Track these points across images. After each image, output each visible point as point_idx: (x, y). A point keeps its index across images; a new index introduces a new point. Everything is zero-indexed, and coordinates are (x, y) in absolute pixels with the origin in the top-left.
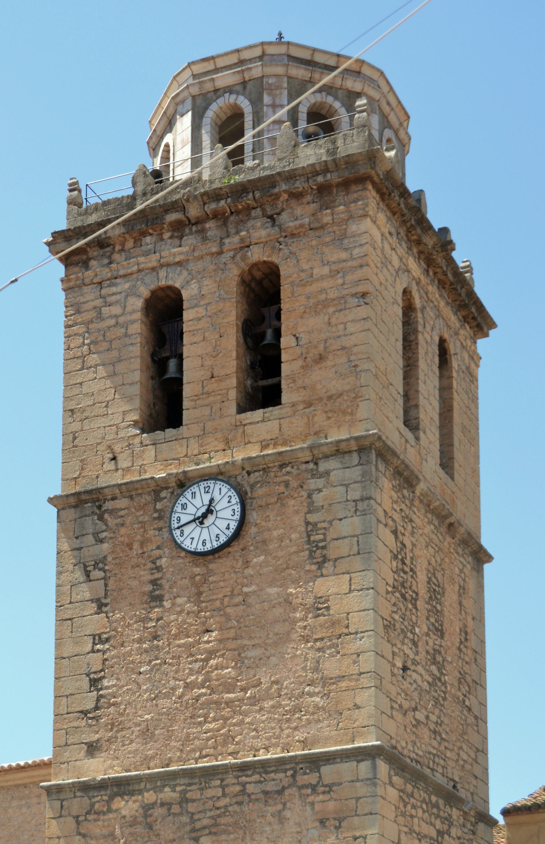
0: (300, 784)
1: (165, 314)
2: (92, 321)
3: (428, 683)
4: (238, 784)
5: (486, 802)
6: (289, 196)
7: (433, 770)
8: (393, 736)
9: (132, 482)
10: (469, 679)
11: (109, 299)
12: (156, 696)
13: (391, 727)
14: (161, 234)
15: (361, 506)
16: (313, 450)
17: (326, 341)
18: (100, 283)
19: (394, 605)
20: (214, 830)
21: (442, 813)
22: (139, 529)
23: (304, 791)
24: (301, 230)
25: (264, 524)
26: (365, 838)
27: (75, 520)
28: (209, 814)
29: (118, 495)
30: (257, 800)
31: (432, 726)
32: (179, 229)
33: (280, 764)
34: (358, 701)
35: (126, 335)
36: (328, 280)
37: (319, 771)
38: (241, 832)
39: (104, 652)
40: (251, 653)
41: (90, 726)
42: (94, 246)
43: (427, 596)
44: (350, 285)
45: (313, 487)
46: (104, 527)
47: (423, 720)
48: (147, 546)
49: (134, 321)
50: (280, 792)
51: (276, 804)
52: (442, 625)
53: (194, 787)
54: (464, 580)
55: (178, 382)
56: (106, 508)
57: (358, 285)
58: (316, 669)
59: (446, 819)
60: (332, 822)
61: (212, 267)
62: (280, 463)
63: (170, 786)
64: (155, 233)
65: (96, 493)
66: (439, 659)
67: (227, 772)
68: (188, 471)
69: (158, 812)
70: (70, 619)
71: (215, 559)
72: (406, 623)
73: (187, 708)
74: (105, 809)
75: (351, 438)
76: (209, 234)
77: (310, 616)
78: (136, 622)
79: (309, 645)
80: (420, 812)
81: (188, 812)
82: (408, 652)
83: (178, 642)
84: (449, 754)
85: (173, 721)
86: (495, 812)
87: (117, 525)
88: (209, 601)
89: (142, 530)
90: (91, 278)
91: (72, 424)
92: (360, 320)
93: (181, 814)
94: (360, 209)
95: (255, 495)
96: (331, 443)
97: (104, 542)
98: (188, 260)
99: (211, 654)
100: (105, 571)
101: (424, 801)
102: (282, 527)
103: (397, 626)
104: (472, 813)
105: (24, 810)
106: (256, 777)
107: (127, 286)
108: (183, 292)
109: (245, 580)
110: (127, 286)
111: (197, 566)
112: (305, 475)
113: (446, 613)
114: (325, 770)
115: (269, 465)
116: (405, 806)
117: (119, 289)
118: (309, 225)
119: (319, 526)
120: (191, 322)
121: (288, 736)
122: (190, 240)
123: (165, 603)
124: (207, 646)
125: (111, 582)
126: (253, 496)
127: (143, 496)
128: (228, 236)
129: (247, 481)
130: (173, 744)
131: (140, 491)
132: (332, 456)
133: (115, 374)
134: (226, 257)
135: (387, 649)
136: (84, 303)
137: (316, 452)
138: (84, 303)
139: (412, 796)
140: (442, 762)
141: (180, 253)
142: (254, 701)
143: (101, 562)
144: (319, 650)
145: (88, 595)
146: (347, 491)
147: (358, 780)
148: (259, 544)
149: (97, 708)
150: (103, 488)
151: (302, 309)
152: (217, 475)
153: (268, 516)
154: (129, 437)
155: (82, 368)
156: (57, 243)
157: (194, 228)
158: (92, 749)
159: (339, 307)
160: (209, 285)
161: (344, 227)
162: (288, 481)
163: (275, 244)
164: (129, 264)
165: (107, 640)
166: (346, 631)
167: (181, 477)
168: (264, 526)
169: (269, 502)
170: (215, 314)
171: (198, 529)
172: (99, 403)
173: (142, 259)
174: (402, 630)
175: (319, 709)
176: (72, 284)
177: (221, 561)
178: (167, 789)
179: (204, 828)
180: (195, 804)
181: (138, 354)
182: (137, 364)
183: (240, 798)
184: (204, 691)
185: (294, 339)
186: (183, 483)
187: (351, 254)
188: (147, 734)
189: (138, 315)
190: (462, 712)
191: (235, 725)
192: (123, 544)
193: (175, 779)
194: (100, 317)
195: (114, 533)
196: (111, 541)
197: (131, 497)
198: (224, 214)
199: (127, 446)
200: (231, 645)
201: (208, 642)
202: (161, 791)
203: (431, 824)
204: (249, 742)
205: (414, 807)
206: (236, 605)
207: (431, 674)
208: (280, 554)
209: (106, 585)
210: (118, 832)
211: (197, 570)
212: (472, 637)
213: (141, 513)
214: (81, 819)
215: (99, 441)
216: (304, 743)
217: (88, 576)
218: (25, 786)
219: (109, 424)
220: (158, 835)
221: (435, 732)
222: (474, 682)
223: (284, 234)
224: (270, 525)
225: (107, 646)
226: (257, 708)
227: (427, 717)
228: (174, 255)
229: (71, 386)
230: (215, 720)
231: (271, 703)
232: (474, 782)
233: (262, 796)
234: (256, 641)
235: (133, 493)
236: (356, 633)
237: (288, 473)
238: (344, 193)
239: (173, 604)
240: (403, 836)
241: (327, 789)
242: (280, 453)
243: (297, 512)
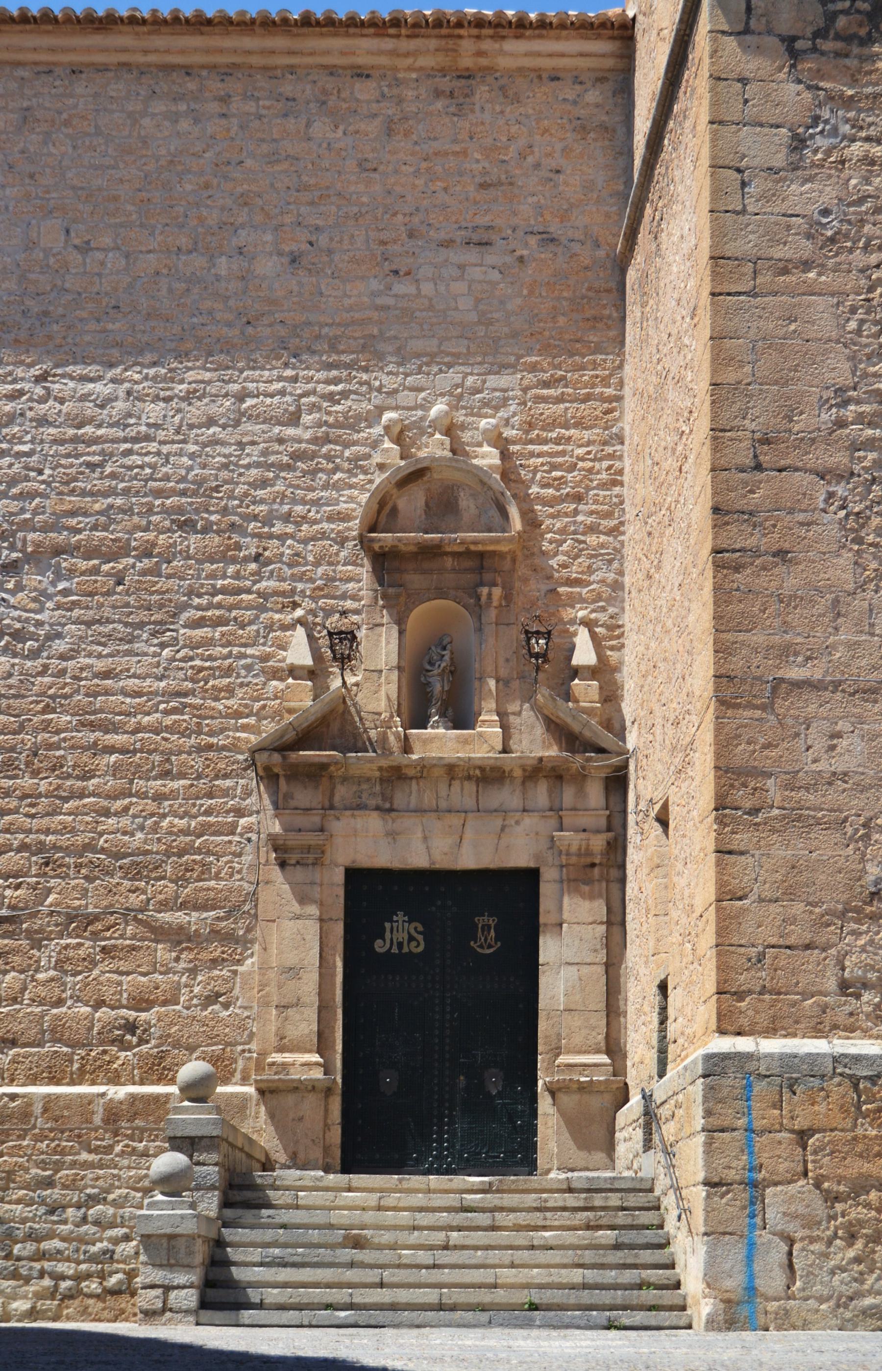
74: (863, 32)
214: (799, 45)
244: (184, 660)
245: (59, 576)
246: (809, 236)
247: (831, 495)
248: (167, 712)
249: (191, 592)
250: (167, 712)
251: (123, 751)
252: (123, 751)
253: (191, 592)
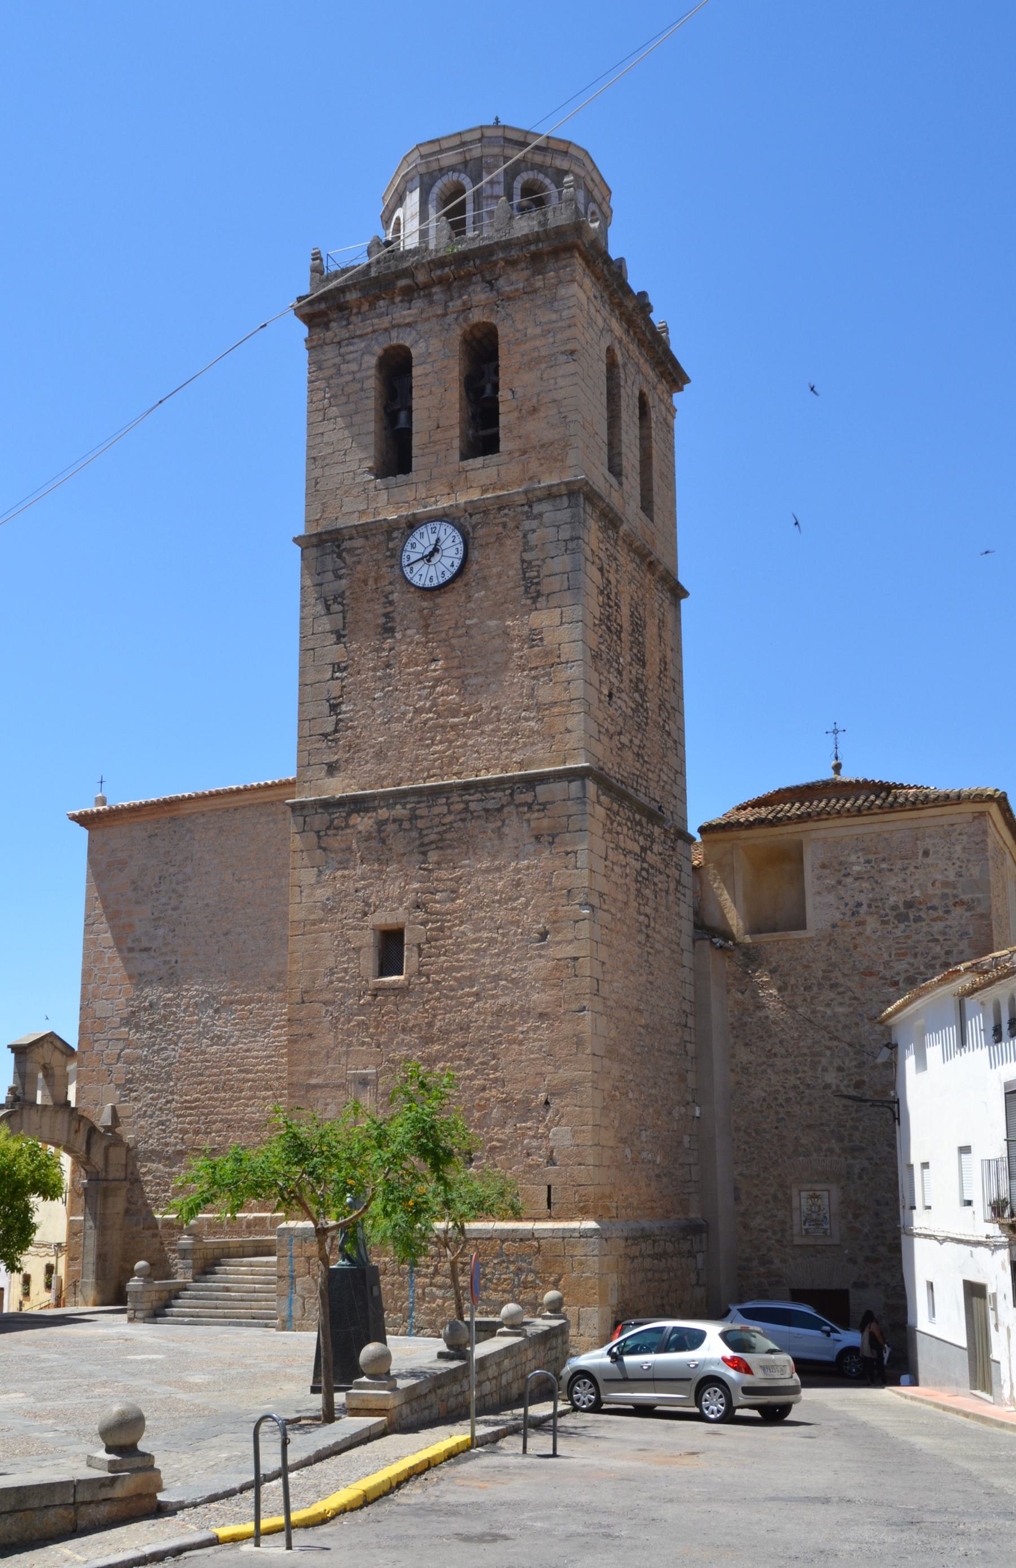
0: (517, 802)
1: (396, 369)
2: (332, 377)
3: (632, 709)
4: (462, 802)
5: (685, 820)
7: (636, 790)
8: (601, 758)
9: (367, 523)
10: (668, 706)
11: (347, 357)
12: (389, 720)
13: (599, 750)
14: (393, 298)
15: (570, 545)
17: (538, 394)
18: (339, 343)
19: (601, 636)
20: (440, 845)
21: (645, 831)
23: (521, 809)
25: (484, 562)
26: (576, 853)
28: (436, 830)
30: (479, 817)
31: (636, 749)
32: (409, 294)
33: (499, 783)
34: (569, 725)
35: (362, 390)
37: (534, 791)
38: (464, 847)
39: (343, 679)
40: (474, 681)
41: (330, 748)
43: (630, 629)
45: (527, 527)
46: (343, 565)
47: (627, 743)
49: (368, 378)
50: (500, 810)
51: (495, 821)
52: (643, 656)
53: (423, 805)
54: (663, 614)
55: (408, 433)
58: (531, 696)
59: (648, 836)
60: (547, 838)
61: (437, 328)
63: (401, 803)
66: (641, 687)
67: (452, 791)
69: (391, 827)
70: (313, 649)
72: (611, 654)
73: (416, 731)
74: (343, 825)
77: (526, 646)
78: (371, 652)
79: (525, 673)
80: (625, 828)
81: (417, 828)
82: (614, 680)
83: (408, 670)
84: (650, 775)
85: (404, 743)
86: (693, 830)
87: (354, 562)
93: (410, 830)
96: (544, 487)
98: (416, 322)
99: (438, 681)
100: (343, 605)
101: (628, 819)
102: (501, 564)
103: (604, 656)
104: (672, 831)
105: (271, 825)
106: (478, 796)
107: (363, 345)
108: (412, 351)
110: (363, 345)
111: (425, 600)
113: (648, 645)
114: (540, 789)
116: (612, 824)
121: (507, 758)
122: (418, 304)
123: (396, 635)
124: (434, 674)
125: (349, 615)
128: (452, 300)
130: (404, 764)
131: (374, 532)
133: (352, 425)
134: (451, 318)
135: (594, 677)
137: (530, 496)
139: (618, 814)
140: (644, 783)
141: (410, 315)
142: (476, 724)
143: (340, 596)
144: (534, 678)
145: (328, 627)
147: (569, 799)
149: (336, 731)
150: (341, 529)
152: (443, 517)
155: (324, 420)
157: (422, 293)
158: (332, 769)
159: (550, 364)
160: (435, 344)
165: (345, 668)
166: (558, 660)
167: (410, 518)
170: (440, 370)
171: (426, 566)
173: (376, 321)
174: (608, 660)
175: (534, 732)
176: (314, 343)
178: (398, 807)
179: (432, 843)
180: (423, 821)
181: (373, 406)
182: (371, 416)
183: (463, 816)
184: (431, 715)
185: (510, 393)
186: (413, 524)
188: (380, 755)
189: (373, 372)
190: (662, 736)
191: (459, 747)
193: (405, 797)
197: (366, 538)
200: (456, 673)
201: (435, 670)
202: (393, 808)
203: (635, 841)
204: (472, 763)
205: (619, 824)
206: (460, 637)
207: (635, 701)
208: (499, 589)
209: (344, 618)
210: (354, 846)
211: (425, 604)
212: (670, 666)
216: (521, 765)
218: (272, 803)
220: (391, 849)
221: (638, 755)
222: (673, 708)
224: (489, 562)
225: (345, 674)
226: (479, 731)
227: (631, 741)
228: (404, 317)
229: (314, 435)
230: (441, 742)
231: (491, 727)
232: (674, 802)
233: (482, 813)
234: (477, 670)
235: (368, 533)
236: (567, 662)
239: (404, 635)
240: (610, 851)
241: (542, 807)
242: (498, 497)
243: (514, 551)
244: (273, 1042)
245: (232, 1014)
246: (323, 910)
247: (327, 1011)
248: (266, 1064)
249: (274, 1016)
250: (266, 1064)
251: (253, 1081)
252: (253, 1081)
253: (274, 1016)
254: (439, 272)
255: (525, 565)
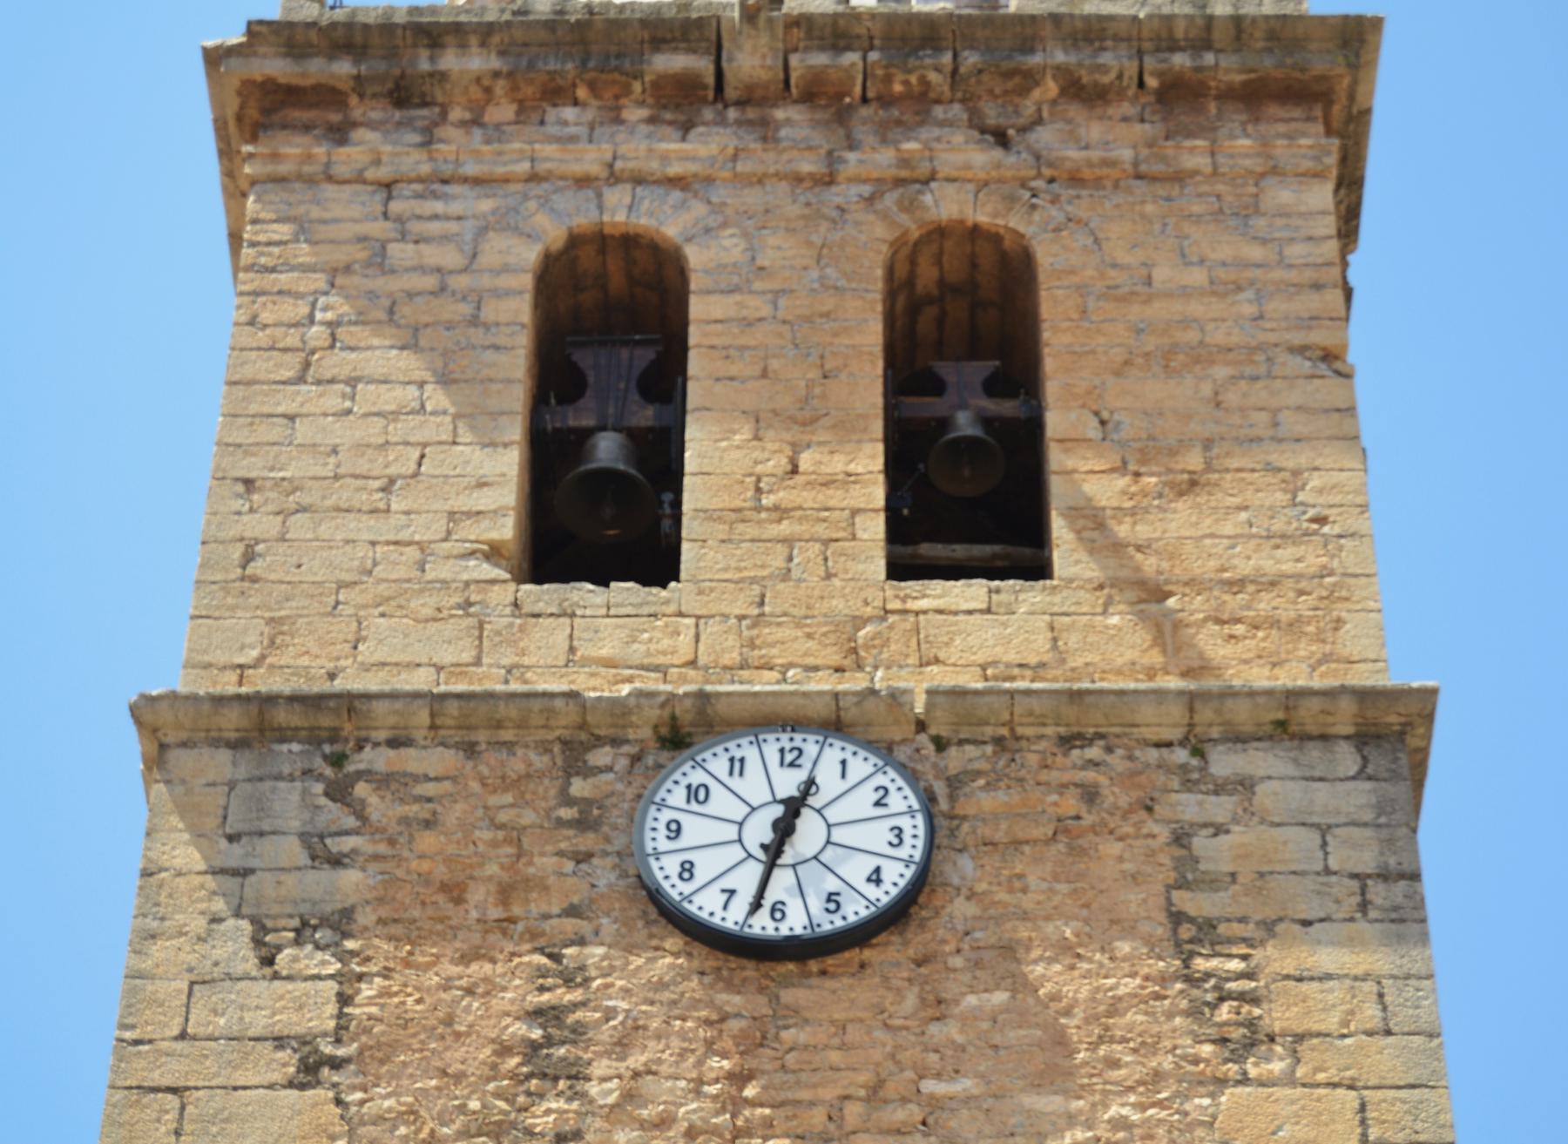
2: (348, 269)
6: (1063, 92)
15: (1377, 892)
16: (1198, 705)
18: (388, 186)
22: (494, 844)
24: (1105, 171)
25: (1002, 896)
27: (232, 785)
29: (419, 735)
32: (683, 102)
35: (474, 321)
36: (1206, 300)
42: (374, 96)
44: (1283, 324)
46: (351, 822)
48: (527, 901)
49: (509, 293)
56: (362, 766)
57: (1310, 328)
62: (1062, 730)
64: (595, 103)
65: (336, 712)
68: (718, 695)
71: (809, 975)
75: (1343, 689)
76: (783, 133)
87: (405, 821)
88: (782, 1104)
89: (510, 850)
90: (359, 166)
91: (245, 518)
92: (1326, 411)
94: (1304, 157)
95: (965, 807)
96: (1269, 693)
97: (345, 866)
98: (709, 180)
100: (344, 957)
107: (486, 205)
109: (933, 1057)
111: (730, 987)
112: (1161, 779)
115: (1020, 730)
117: (455, 208)
118: (1136, 164)
119: (1222, 929)
120: (719, 327)
126: (959, 811)
127: (520, 752)
129: (935, 766)
131: (507, 735)
132: (1259, 739)
134: (847, 194)
136: (324, 222)
138: (324, 222)
141: (686, 158)
143: (325, 922)
146: (1324, 844)
148: (987, 955)
150: (368, 697)
151: (1118, 355)
153: (1020, 876)
154: (467, 584)
155: (301, 379)
156: (255, 54)
157: (732, 113)
159: (1248, 370)
161: (1252, 190)
162: (1096, 785)
163: (1020, 191)
164: (500, 153)
168: (1005, 905)
169: (1021, 835)
170: (808, 319)
172: (356, 477)
173: (550, 150)
177: (829, 983)
185: (1094, 422)
187: (1280, 253)
192: (427, 883)
194: (381, 265)
195: (392, 842)
196: (373, 867)
197: (470, 749)
198: (840, 96)
199: (459, 606)
209: (344, 1000)
213: (509, 798)
215: (347, 577)
217: (268, 961)
219: (392, 537)
223: (1047, 172)
224: (1028, 902)
228: (665, 158)
235: (482, 736)
237: (1095, 764)
238: (1244, 117)
254: (820, 59)
255: (1186, 932)
